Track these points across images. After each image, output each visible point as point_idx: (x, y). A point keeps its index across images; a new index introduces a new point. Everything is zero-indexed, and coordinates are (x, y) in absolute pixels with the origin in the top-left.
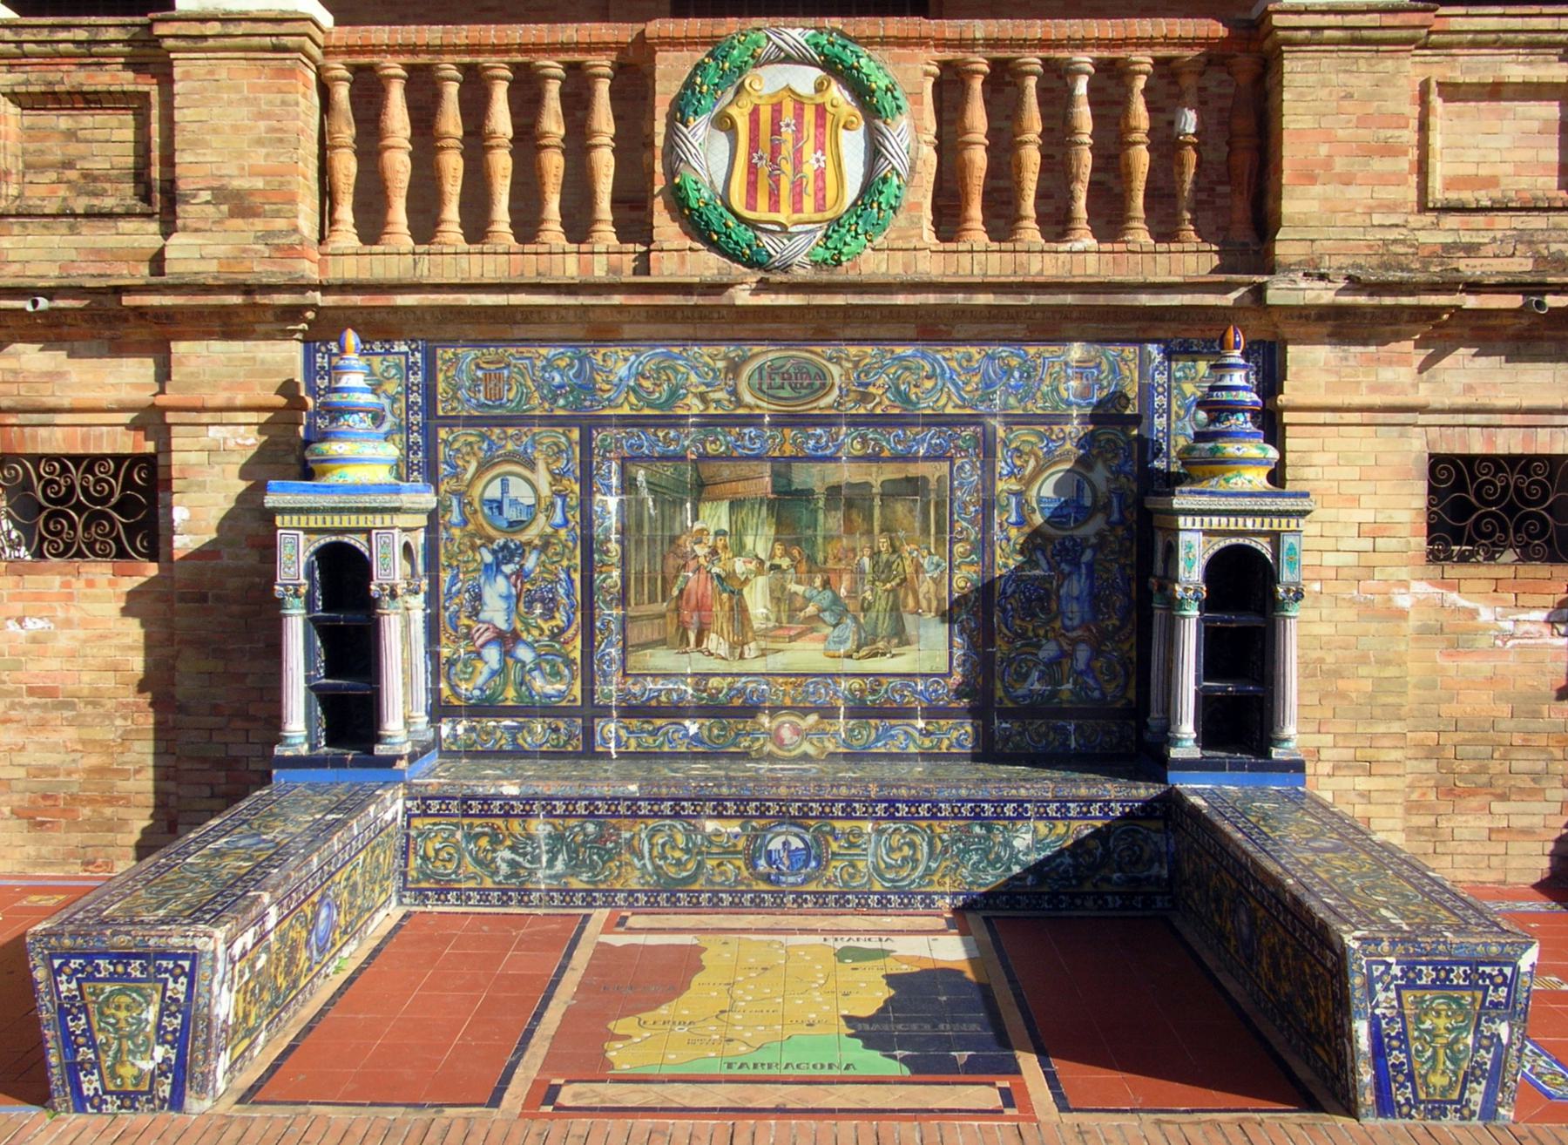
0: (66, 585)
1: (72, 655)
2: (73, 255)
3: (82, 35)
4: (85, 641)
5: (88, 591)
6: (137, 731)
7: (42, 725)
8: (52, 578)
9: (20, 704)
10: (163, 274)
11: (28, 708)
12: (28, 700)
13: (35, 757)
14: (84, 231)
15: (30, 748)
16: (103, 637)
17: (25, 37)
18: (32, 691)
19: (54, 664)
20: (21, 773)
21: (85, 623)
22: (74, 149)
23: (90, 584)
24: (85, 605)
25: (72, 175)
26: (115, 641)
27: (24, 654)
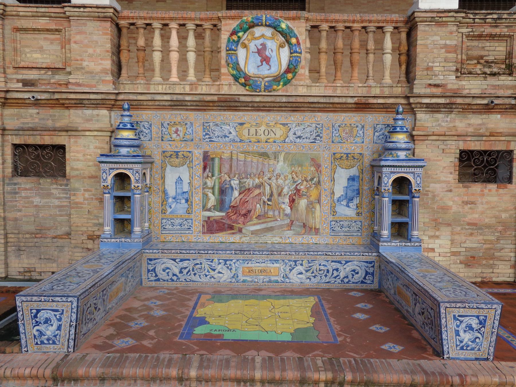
0: (482, 191)
1: (482, 213)
2: (486, 87)
3: (495, 16)
4: (487, 209)
5: (490, 193)
6: (502, 237)
7: (471, 234)
8: (477, 188)
9: (465, 228)
10: (413, 93)
11: (467, 229)
12: (467, 227)
13: (468, 244)
14: (488, 79)
15: (467, 242)
16: (493, 208)
17: (477, 17)
18: (469, 224)
19: (476, 216)
20: (464, 250)
21: (487, 203)
22: (483, 53)
23: (490, 190)
24: (488, 198)
25: (482, 61)
26: (497, 209)
27: (467, 213)
